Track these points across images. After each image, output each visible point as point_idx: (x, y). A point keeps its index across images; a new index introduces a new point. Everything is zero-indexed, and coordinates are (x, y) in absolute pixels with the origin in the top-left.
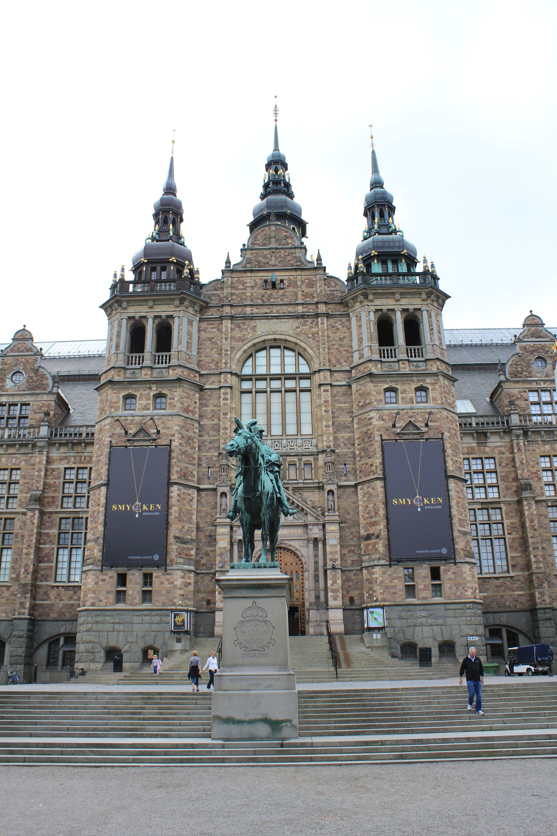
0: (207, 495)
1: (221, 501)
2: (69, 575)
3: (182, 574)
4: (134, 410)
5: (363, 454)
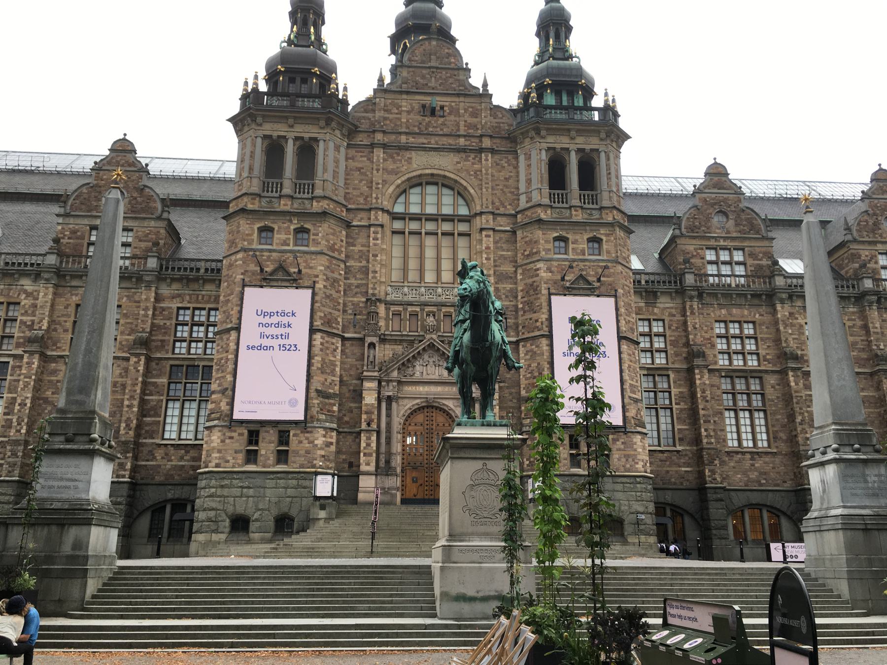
0: (352, 345)
1: (369, 352)
2: (180, 431)
3: (324, 433)
4: (271, 244)
5: (527, 308)
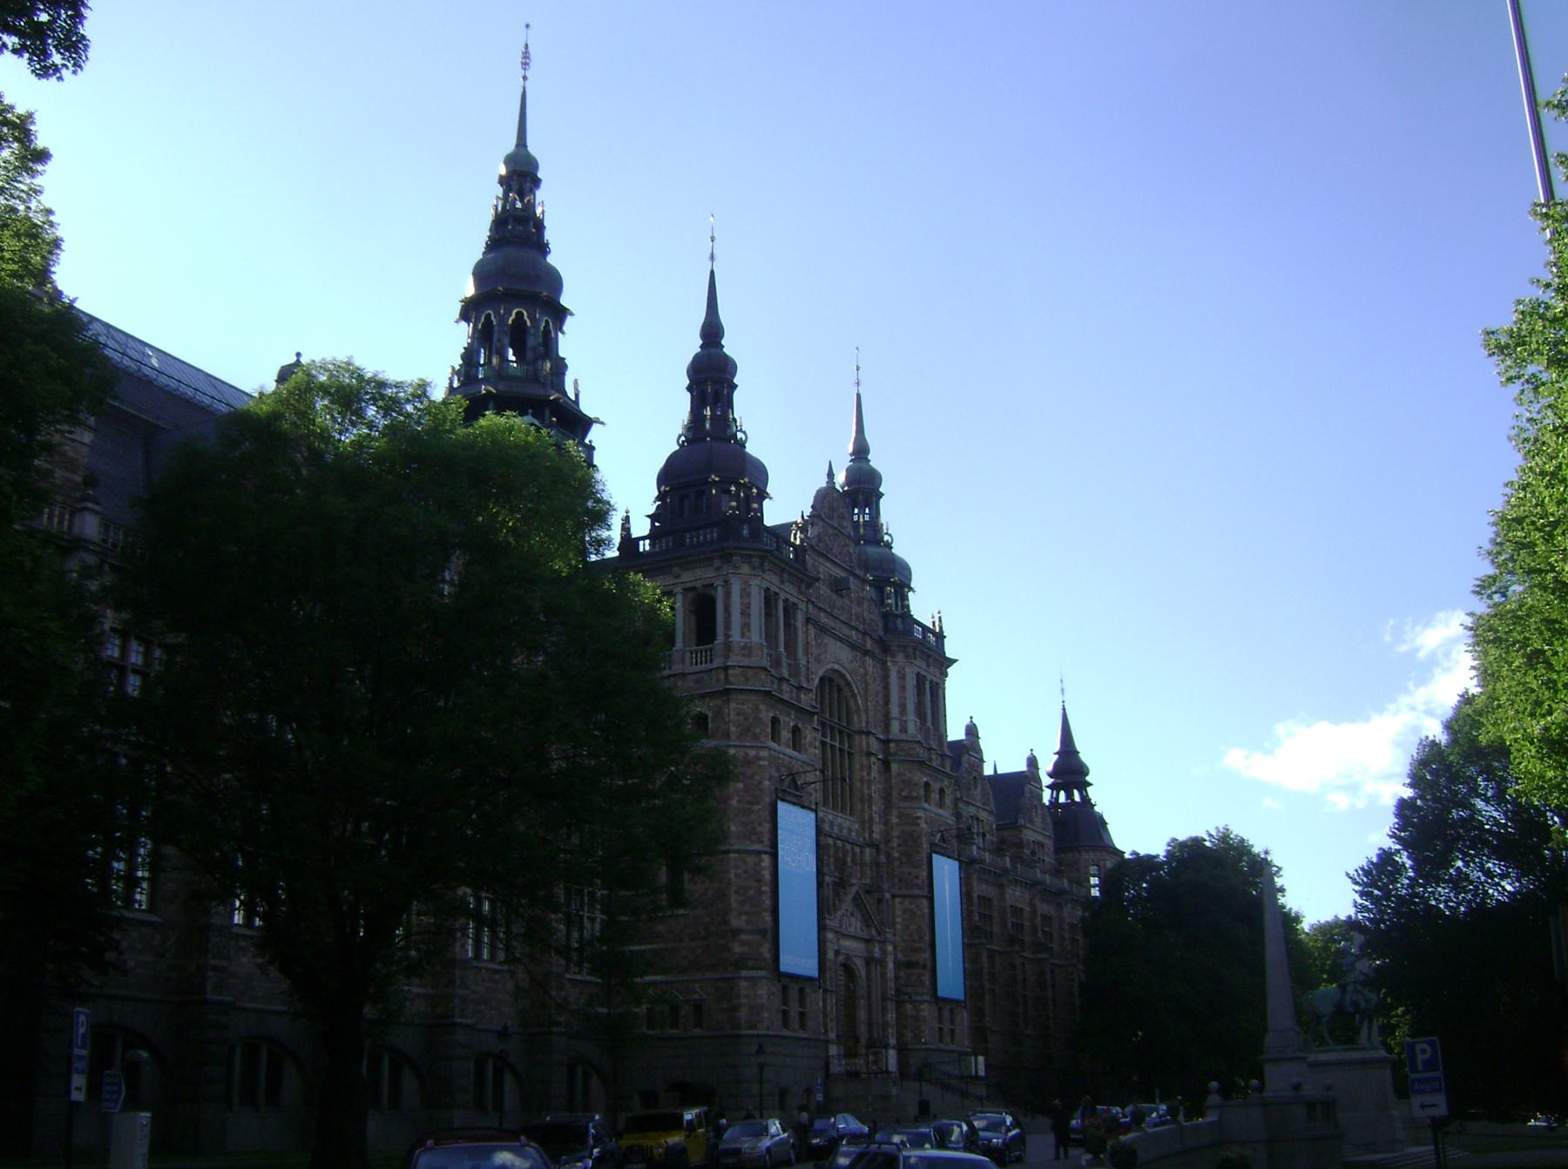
5: (904, 859)
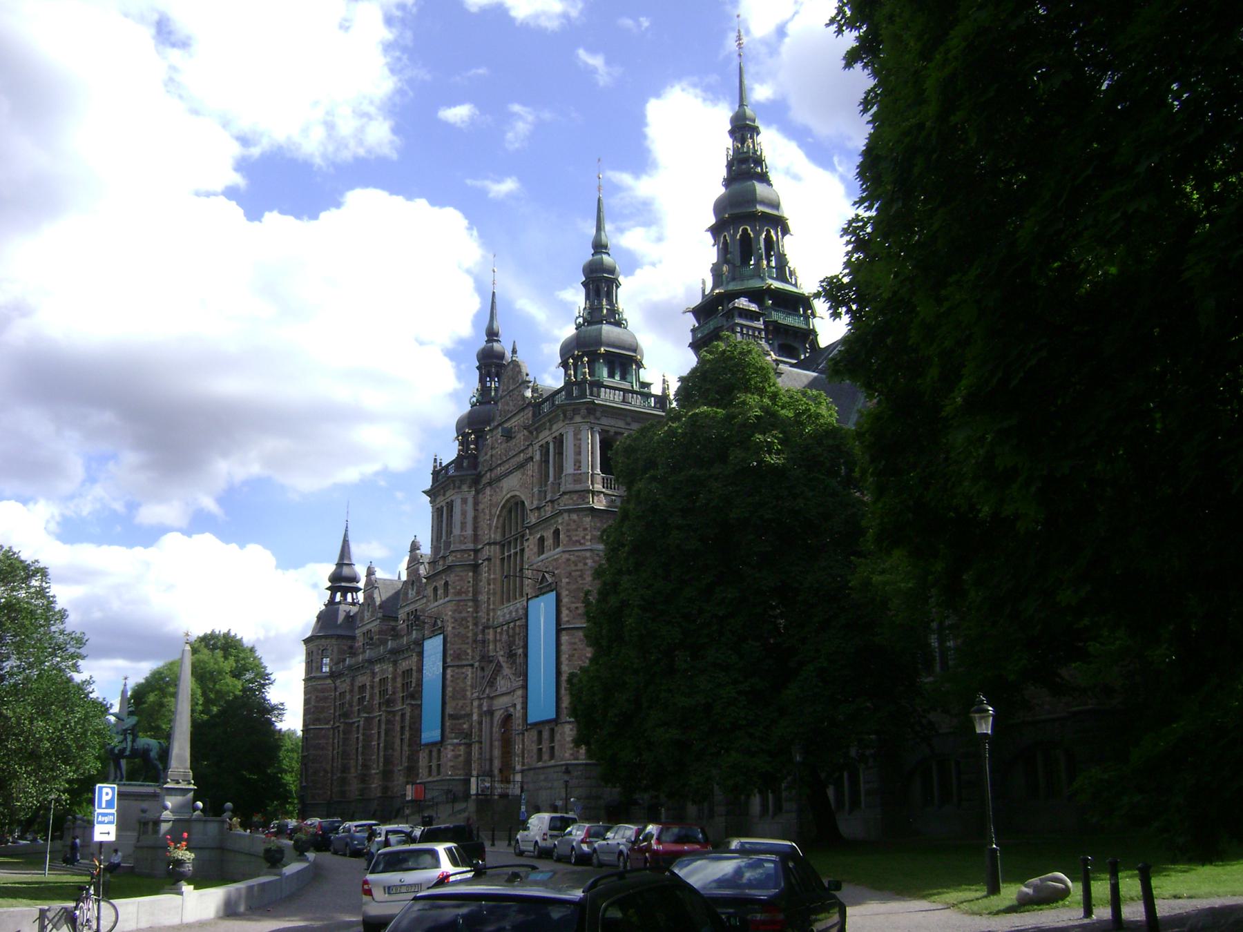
3: (452, 748)
